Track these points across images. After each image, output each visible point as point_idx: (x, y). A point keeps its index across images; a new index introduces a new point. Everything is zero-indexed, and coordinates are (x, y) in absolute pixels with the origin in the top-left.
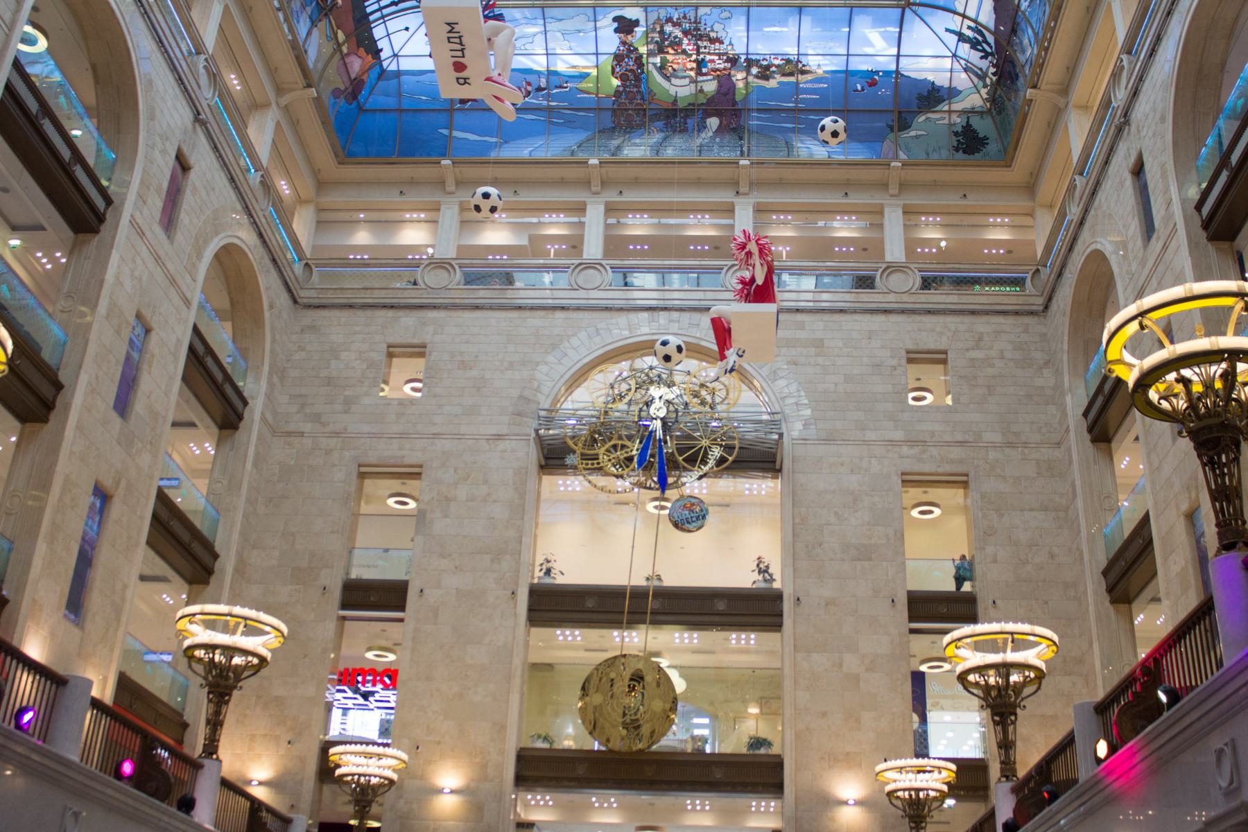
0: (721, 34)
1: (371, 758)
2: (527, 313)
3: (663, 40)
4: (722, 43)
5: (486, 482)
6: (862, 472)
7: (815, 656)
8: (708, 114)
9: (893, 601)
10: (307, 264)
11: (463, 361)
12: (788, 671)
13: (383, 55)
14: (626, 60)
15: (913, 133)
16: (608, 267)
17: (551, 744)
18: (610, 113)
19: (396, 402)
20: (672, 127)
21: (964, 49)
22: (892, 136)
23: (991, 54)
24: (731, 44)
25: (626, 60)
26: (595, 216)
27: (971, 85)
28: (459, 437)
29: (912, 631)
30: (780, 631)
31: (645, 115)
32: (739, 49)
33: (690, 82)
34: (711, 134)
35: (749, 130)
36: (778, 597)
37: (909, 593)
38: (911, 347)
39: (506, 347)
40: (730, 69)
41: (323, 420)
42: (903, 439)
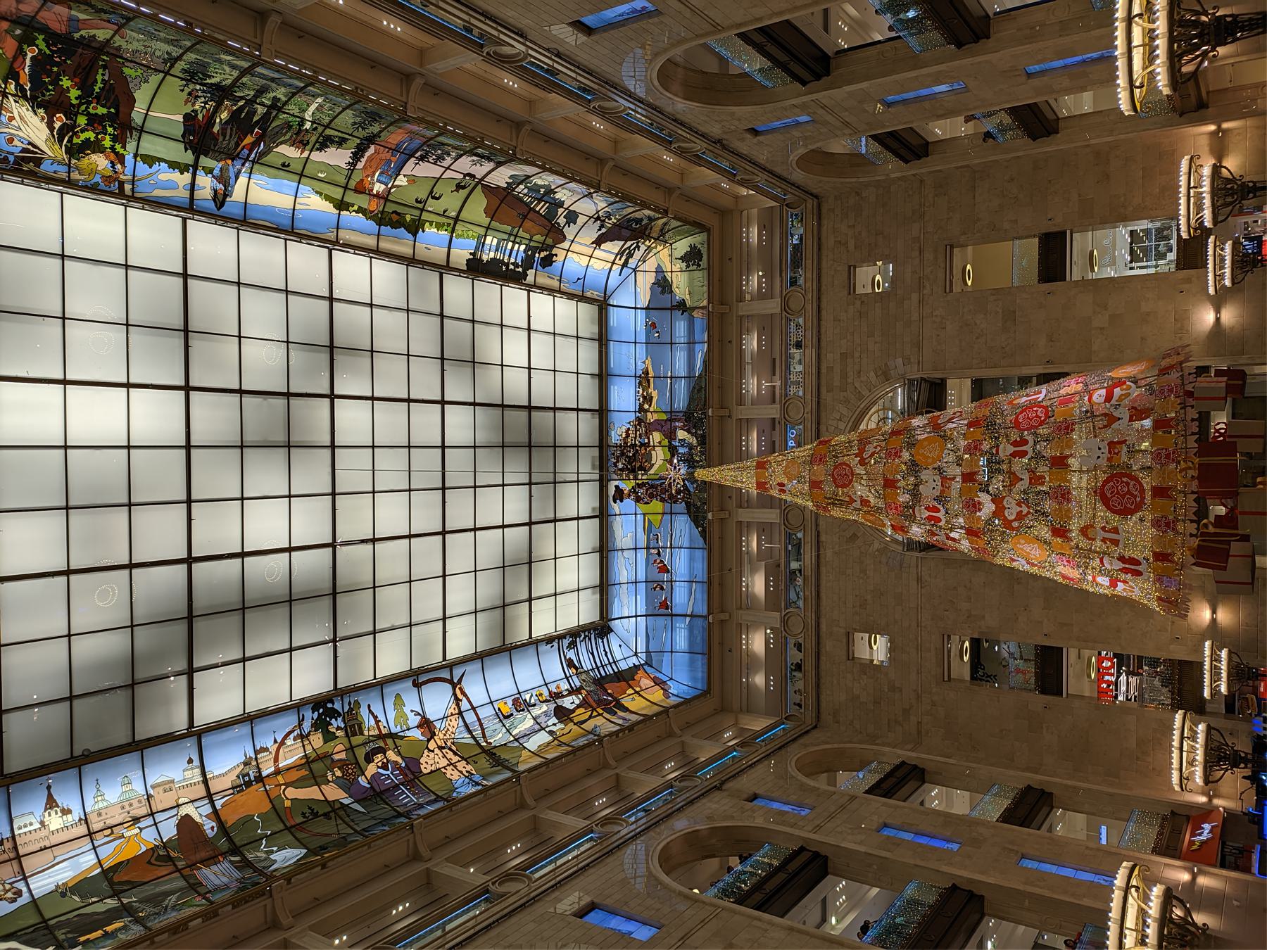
0: (624, 429)
6: (944, 321)
10: (785, 719)
11: (860, 605)
13: (637, 663)
15: (688, 297)
21: (632, 263)
23: (638, 243)
24: (629, 423)
32: (632, 417)
39: (849, 575)
41: (908, 707)
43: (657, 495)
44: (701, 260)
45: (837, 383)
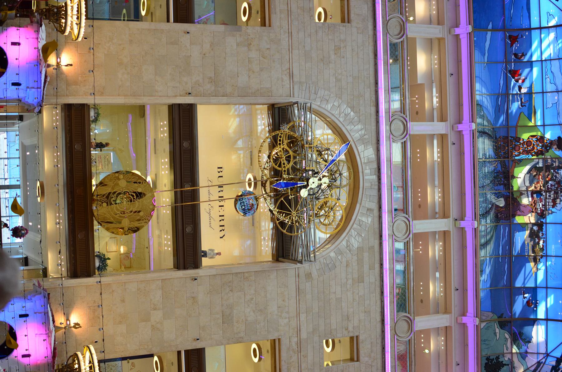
1: (77, 18)
2: (373, 88)
3: (554, 169)
4: (553, 207)
5: (261, 70)
6: (279, 314)
7: (159, 293)
8: (506, 199)
9: (198, 339)
12: (149, 276)
14: (541, 145)
15: (497, 330)
16: (405, 139)
17: (93, 121)
18: (506, 135)
19: (311, 6)
20: (498, 176)
22: (496, 317)
24: (552, 212)
25: (541, 145)
26: (439, 128)
27: (529, 366)
28: (290, 49)
29: (179, 353)
30: (174, 267)
31: (505, 158)
32: (549, 218)
33: (527, 187)
34: (494, 201)
35: (497, 225)
36: (196, 265)
37: (203, 349)
38: (361, 338)
40: (536, 212)
42: (301, 338)
43: (523, 144)
44: (486, 364)
45: (366, 255)
